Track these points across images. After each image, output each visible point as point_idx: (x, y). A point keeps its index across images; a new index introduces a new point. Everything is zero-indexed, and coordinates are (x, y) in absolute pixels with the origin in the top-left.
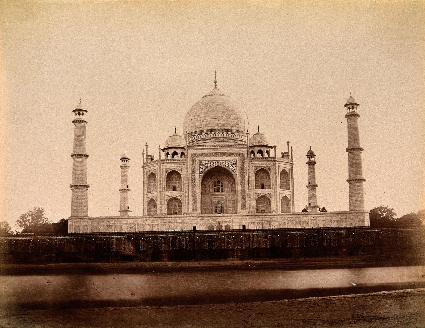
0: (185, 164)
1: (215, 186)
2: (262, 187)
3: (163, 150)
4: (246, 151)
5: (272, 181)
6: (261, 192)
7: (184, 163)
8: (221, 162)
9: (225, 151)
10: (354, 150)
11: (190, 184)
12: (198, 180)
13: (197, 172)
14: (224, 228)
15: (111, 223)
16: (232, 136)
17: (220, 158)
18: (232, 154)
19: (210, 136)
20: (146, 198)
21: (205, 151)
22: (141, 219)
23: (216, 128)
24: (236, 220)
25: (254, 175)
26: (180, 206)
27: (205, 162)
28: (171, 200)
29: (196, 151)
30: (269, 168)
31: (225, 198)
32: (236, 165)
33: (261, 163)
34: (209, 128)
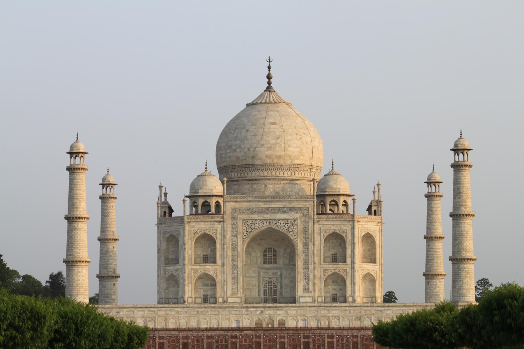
0: (222, 223)
1: (265, 255)
2: (334, 259)
3: (186, 197)
4: (312, 206)
5: (349, 252)
6: (331, 268)
7: (220, 222)
8: (275, 222)
11: (229, 253)
12: (241, 247)
13: (239, 236)
14: (276, 325)
15: (121, 313)
16: (293, 174)
17: (273, 217)
18: (291, 210)
19: (259, 174)
20: (162, 272)
21: (253, 205)
22: (163, 309)
23: (269, 161)
25: (323, 242)
26: (214, 285)
27: (250, 221)
28: (200, 278)
29: (237, 205)
30: (345, 232)
31: (279, 274)
32: (295, 227)
33: (333, 225)
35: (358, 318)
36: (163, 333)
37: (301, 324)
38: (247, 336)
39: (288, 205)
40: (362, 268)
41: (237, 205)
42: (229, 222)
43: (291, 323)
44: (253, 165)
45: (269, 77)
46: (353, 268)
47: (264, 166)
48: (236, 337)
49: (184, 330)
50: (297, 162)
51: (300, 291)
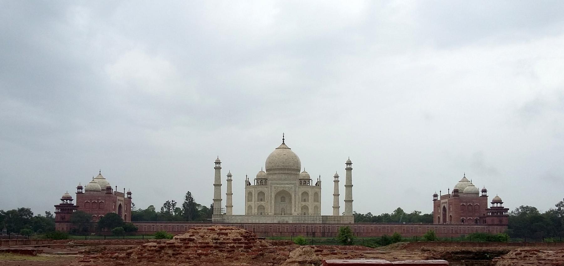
4: (298, 182)
6: (304, 203)
10: (349, 186)
18: (291, 184)
21: (277, 182)
24: (291, 218)
43: (291, 222)
45: (283, 139)
51: (293, 211)
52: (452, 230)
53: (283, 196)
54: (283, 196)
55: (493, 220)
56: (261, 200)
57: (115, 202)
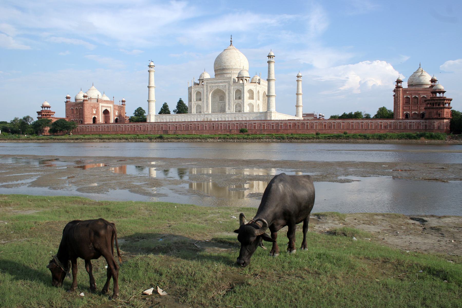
2: (240, 98)
5: (242, 96)
6: (237, 101)
9: (221, 81)
17: (219, 85)
18: (224, 82)
21: (212, 81)
29: (208, 81)
34: (221, 68)
35: (235, 118)
36: (170, 123)
37: (216, 120)
38: (195, 124)
39: (223, 81)
40: (247, 101)
41: (208, 81)
42: (205, 87)
43: (213, 120)
44: (220, 69)
45: (231, 41)
46: (243, 101)
47: (224, 69)
48: (191, 124)
49: (176, 122)
50: (234, 67)
52: (381, 125)
53: (220, 95)
54: (220, 95)
55: (430, 113)
56: (200, 100)
57: (97, 109)
